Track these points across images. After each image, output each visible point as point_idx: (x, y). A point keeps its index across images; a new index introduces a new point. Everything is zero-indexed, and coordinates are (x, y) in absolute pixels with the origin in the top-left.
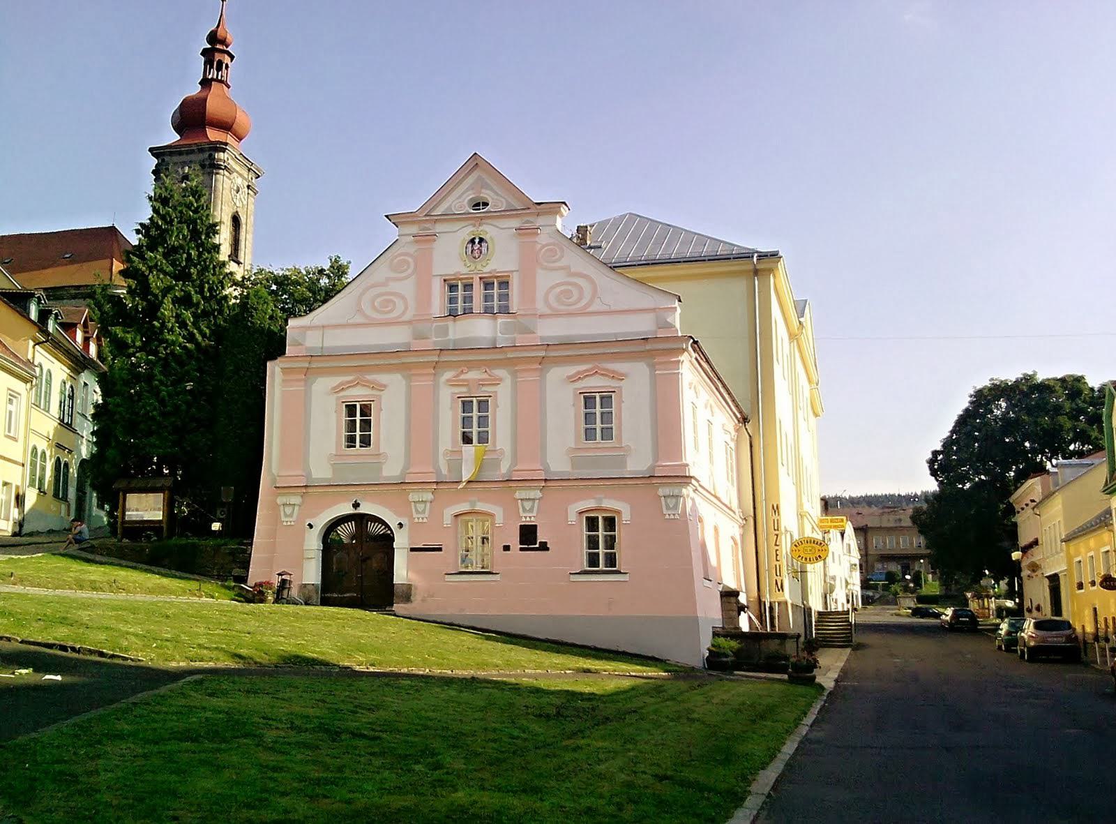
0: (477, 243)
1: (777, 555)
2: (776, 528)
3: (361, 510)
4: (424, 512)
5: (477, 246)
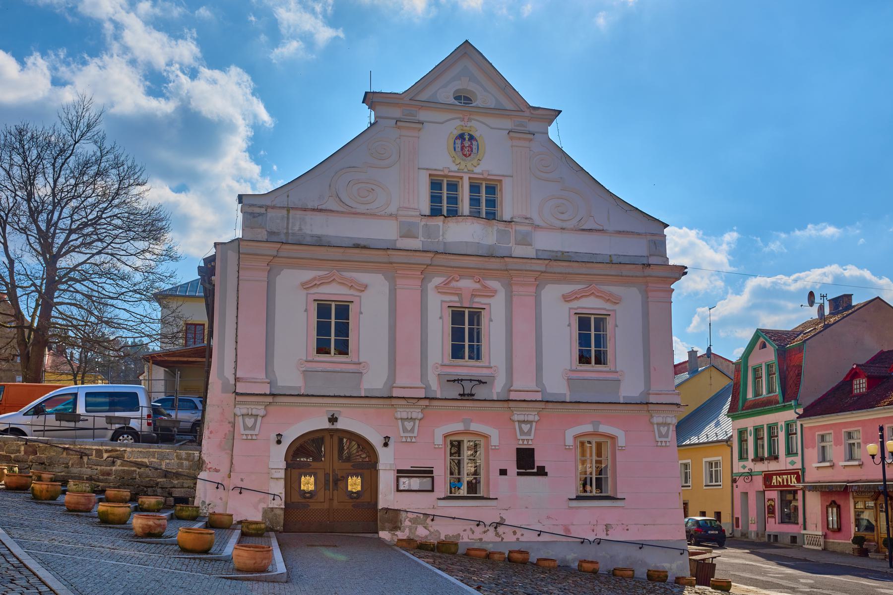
0: (467, 139)
3: (339, 425)
4: (412, 430)
5: (467, 143)
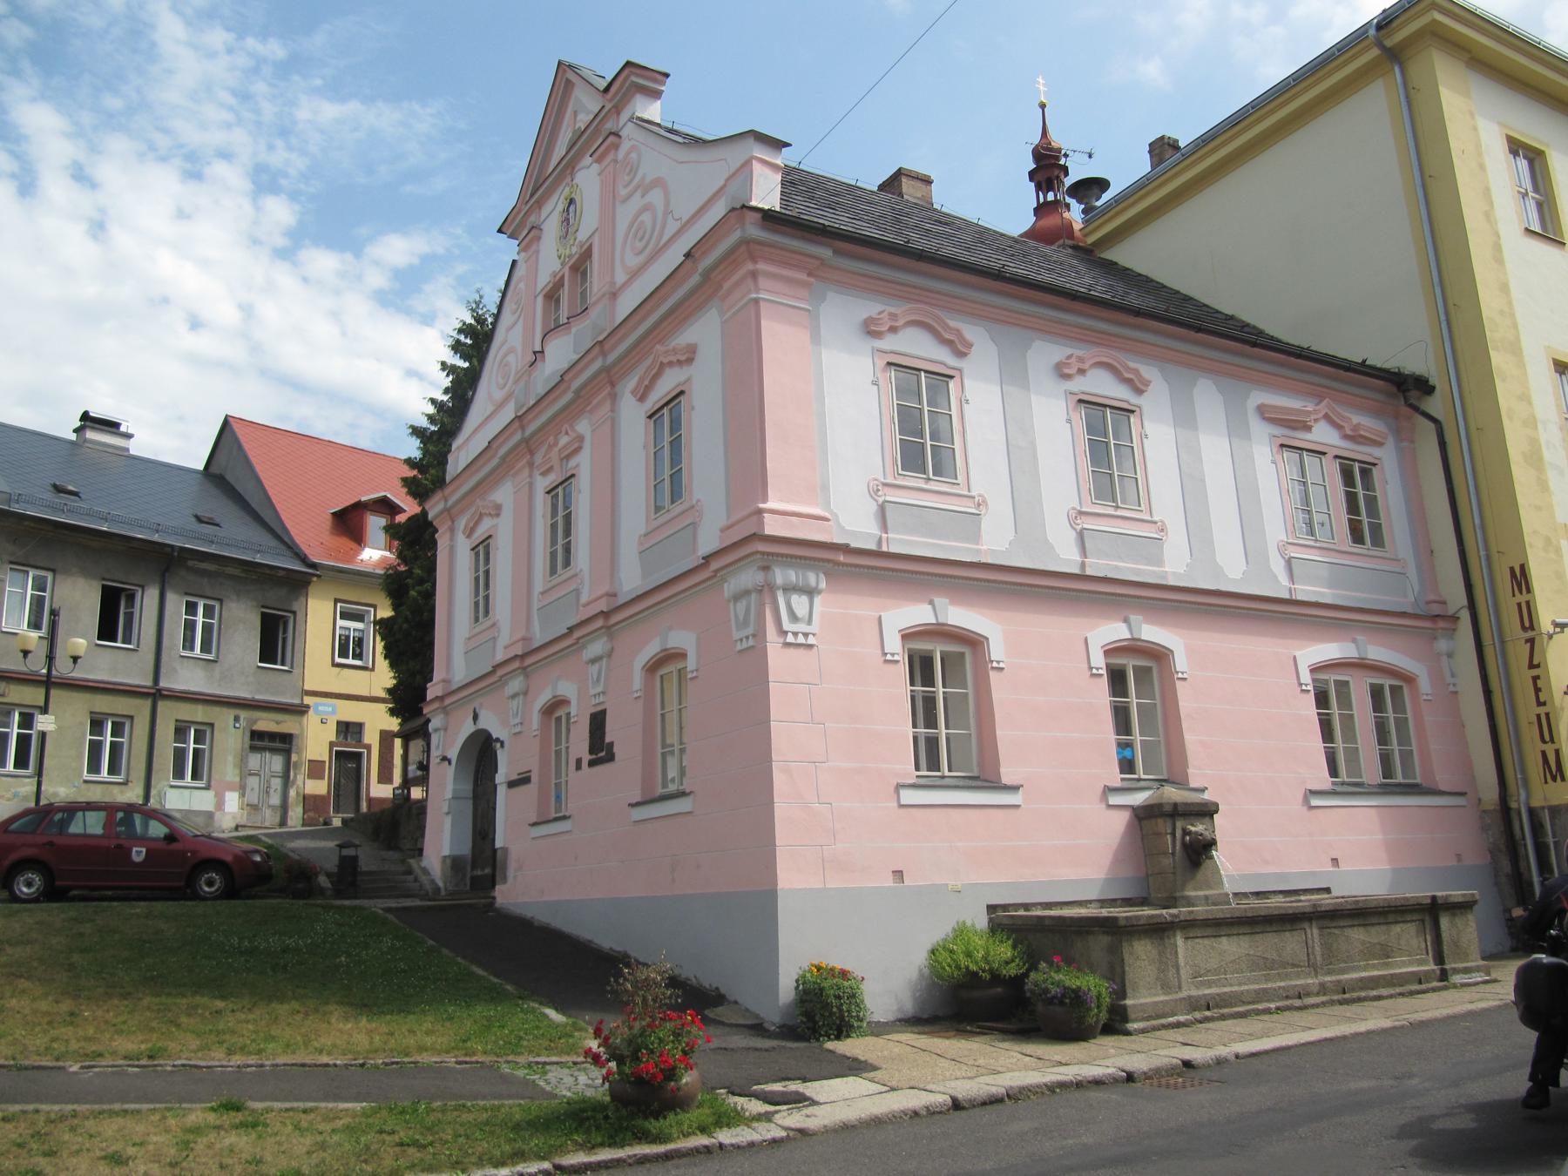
1: (1537, 690)
2: (1527, 624)
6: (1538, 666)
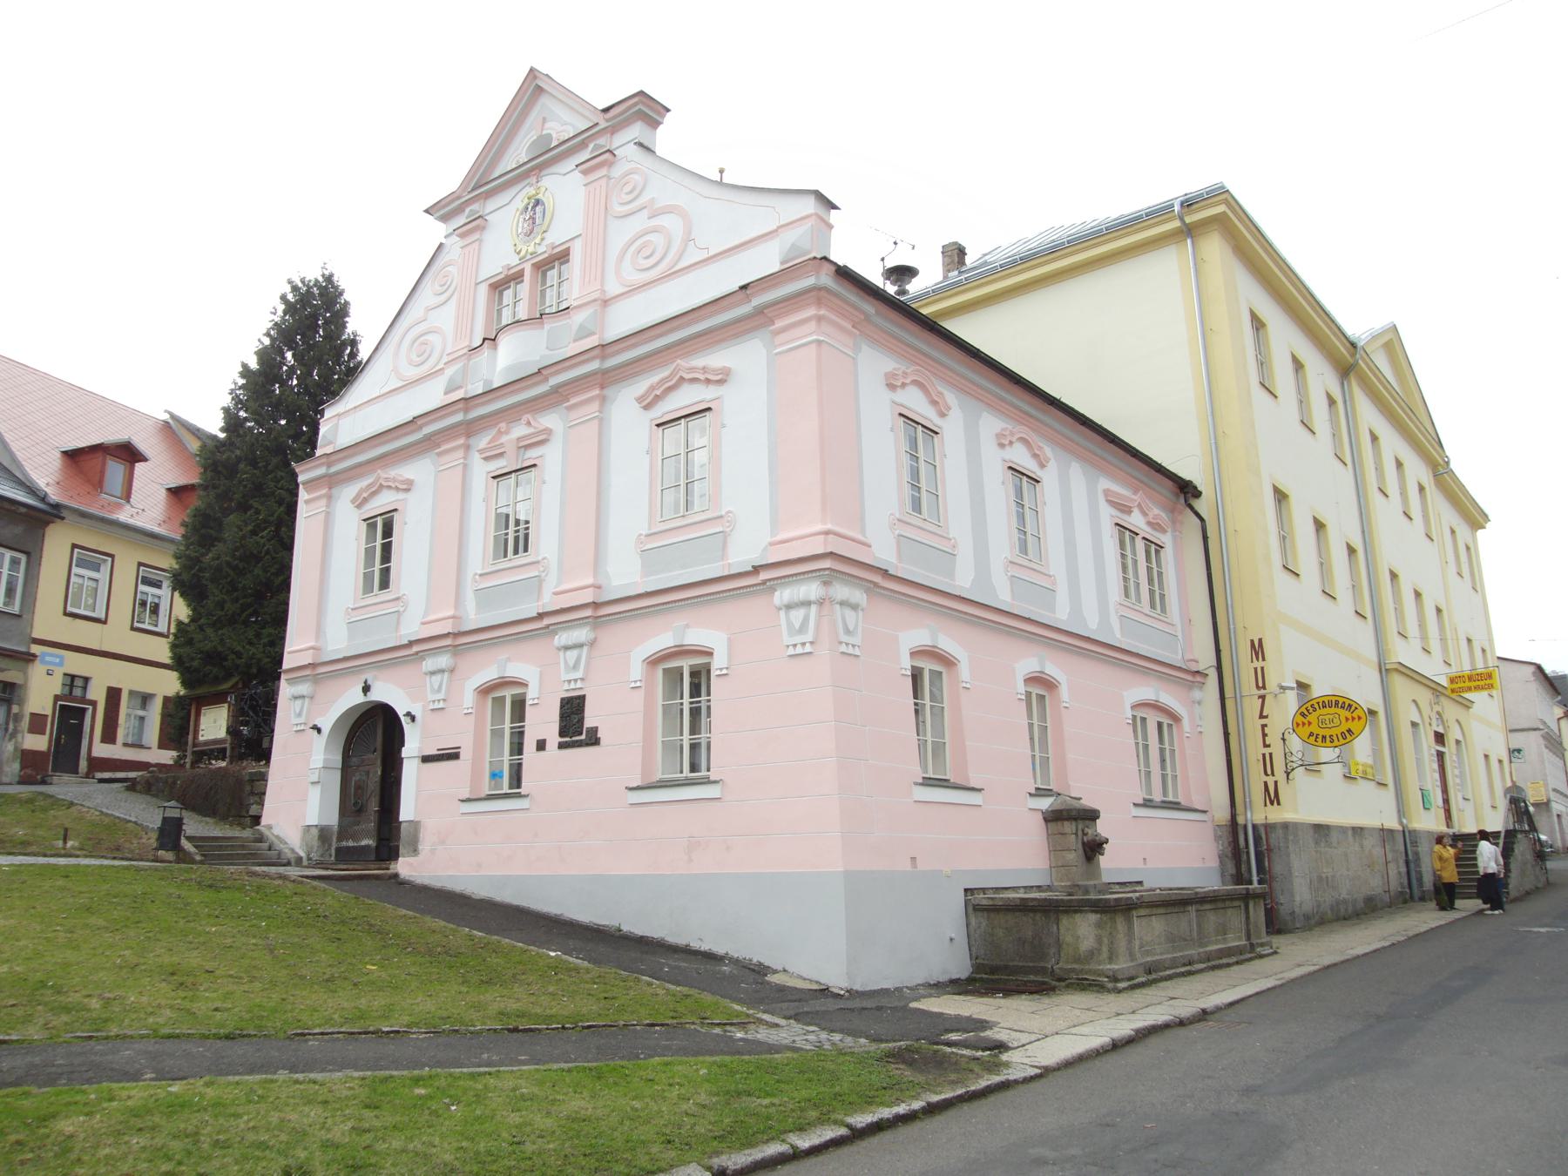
1: (1264, 735)
2: (1261, 685)
6: (1266, 717)
